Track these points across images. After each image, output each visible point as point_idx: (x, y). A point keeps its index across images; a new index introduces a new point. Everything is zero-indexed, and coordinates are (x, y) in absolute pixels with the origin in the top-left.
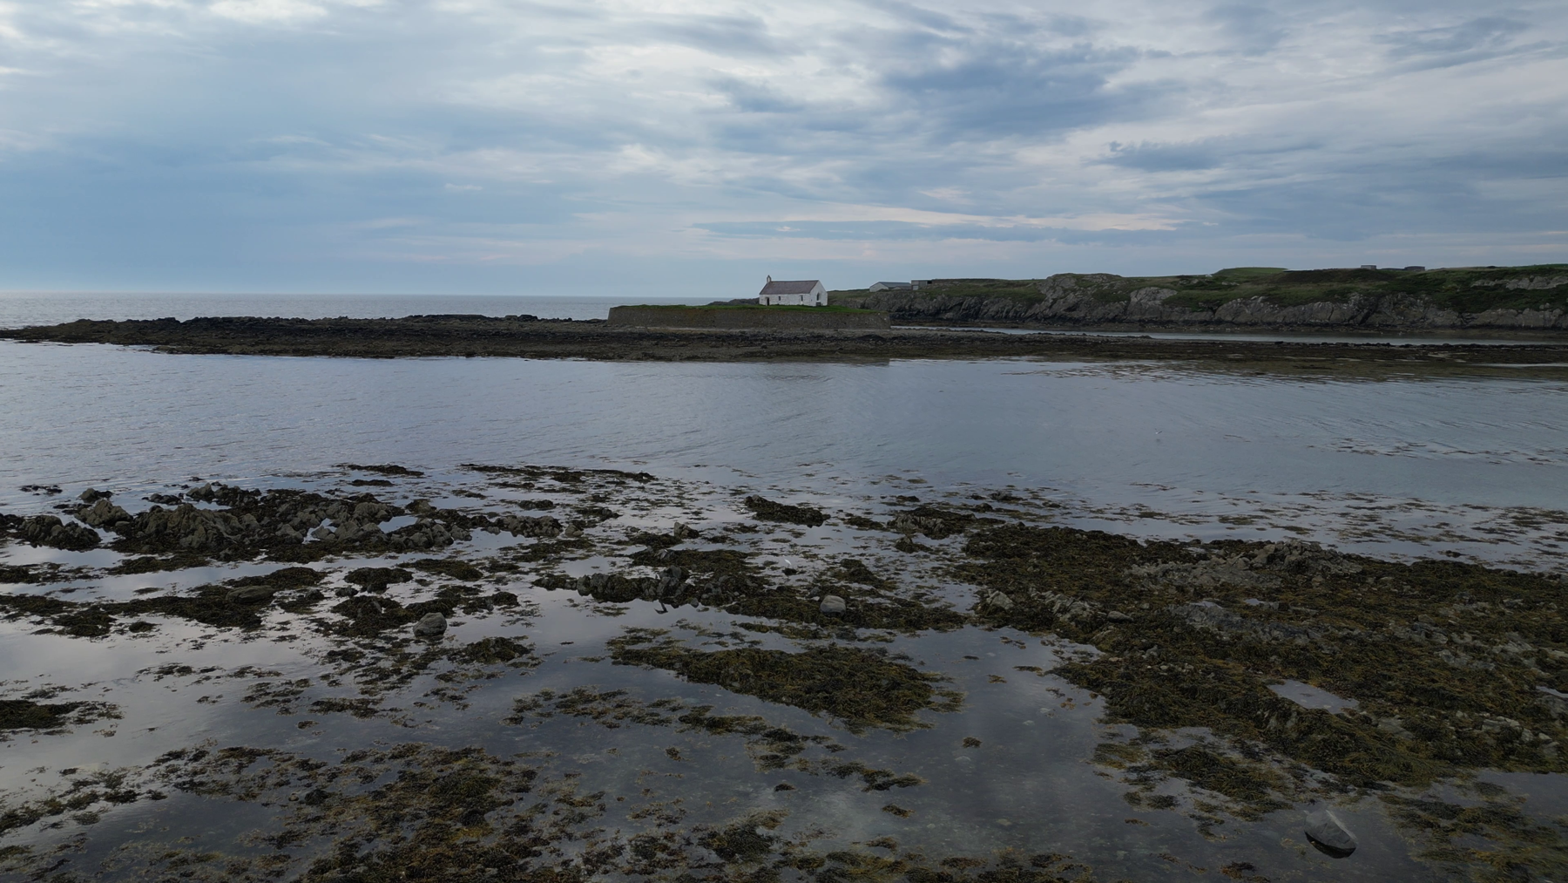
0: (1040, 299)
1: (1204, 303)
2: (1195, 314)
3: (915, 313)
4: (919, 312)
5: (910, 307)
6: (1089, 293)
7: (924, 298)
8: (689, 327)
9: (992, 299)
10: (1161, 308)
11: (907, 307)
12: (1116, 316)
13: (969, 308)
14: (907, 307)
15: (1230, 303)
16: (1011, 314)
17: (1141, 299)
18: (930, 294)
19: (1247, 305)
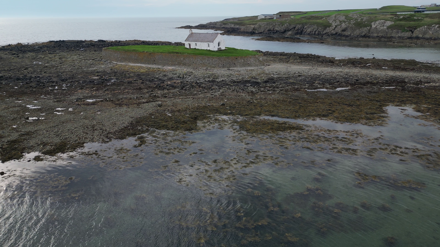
0: (329, 25)
1: (408, 28)
2: (403, 33)
4: (277, 31)
5: (273, 29)
6: (352, 23)
7: (279, 25)
8: (141, 63)
9: (308, 26)
10: (387, 30)
11: (272, 29)
12: (365, 34)
14: (272, 29)
15: (421, 28)
16: (317, 33)
17: (377, 26)
18: (282, 23)
19: (430, 29)
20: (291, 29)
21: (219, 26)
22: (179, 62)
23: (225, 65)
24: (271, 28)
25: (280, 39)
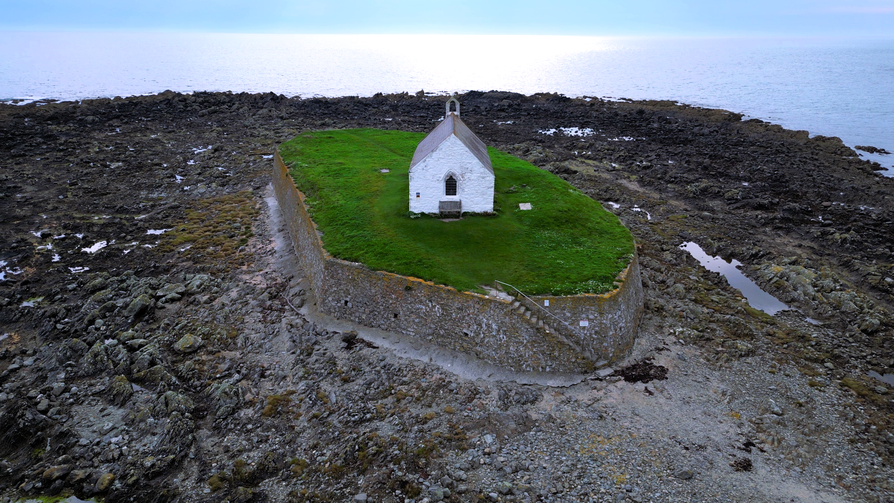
23: (349, 305)
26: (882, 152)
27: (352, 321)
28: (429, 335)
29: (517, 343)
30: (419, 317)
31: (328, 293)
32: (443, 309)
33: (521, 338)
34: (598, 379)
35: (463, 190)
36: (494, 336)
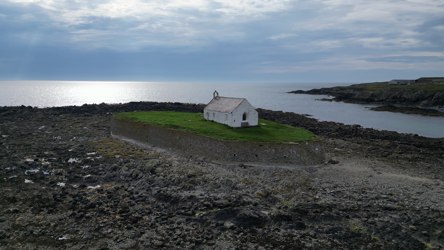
3: (403, 100)
5: (400, 96)
8: (134, 139)
11: (398, 97)
13: (438, 98)
14: (398, 97)
18: (413, 89)
20: (427, 97)
21: (335, 92)
22: (173, 143)
24: (397, 95)
25: (405, 110)
26: (309, 115)
27: (238, 161)
28: (271, 160)
29: (303, 156)
30: (266, 154)
31: (226, 153)
32: (275, 150)
33: (304, 154)
34: (325, 164)
35: (249, 118)
36: (296, 155)
